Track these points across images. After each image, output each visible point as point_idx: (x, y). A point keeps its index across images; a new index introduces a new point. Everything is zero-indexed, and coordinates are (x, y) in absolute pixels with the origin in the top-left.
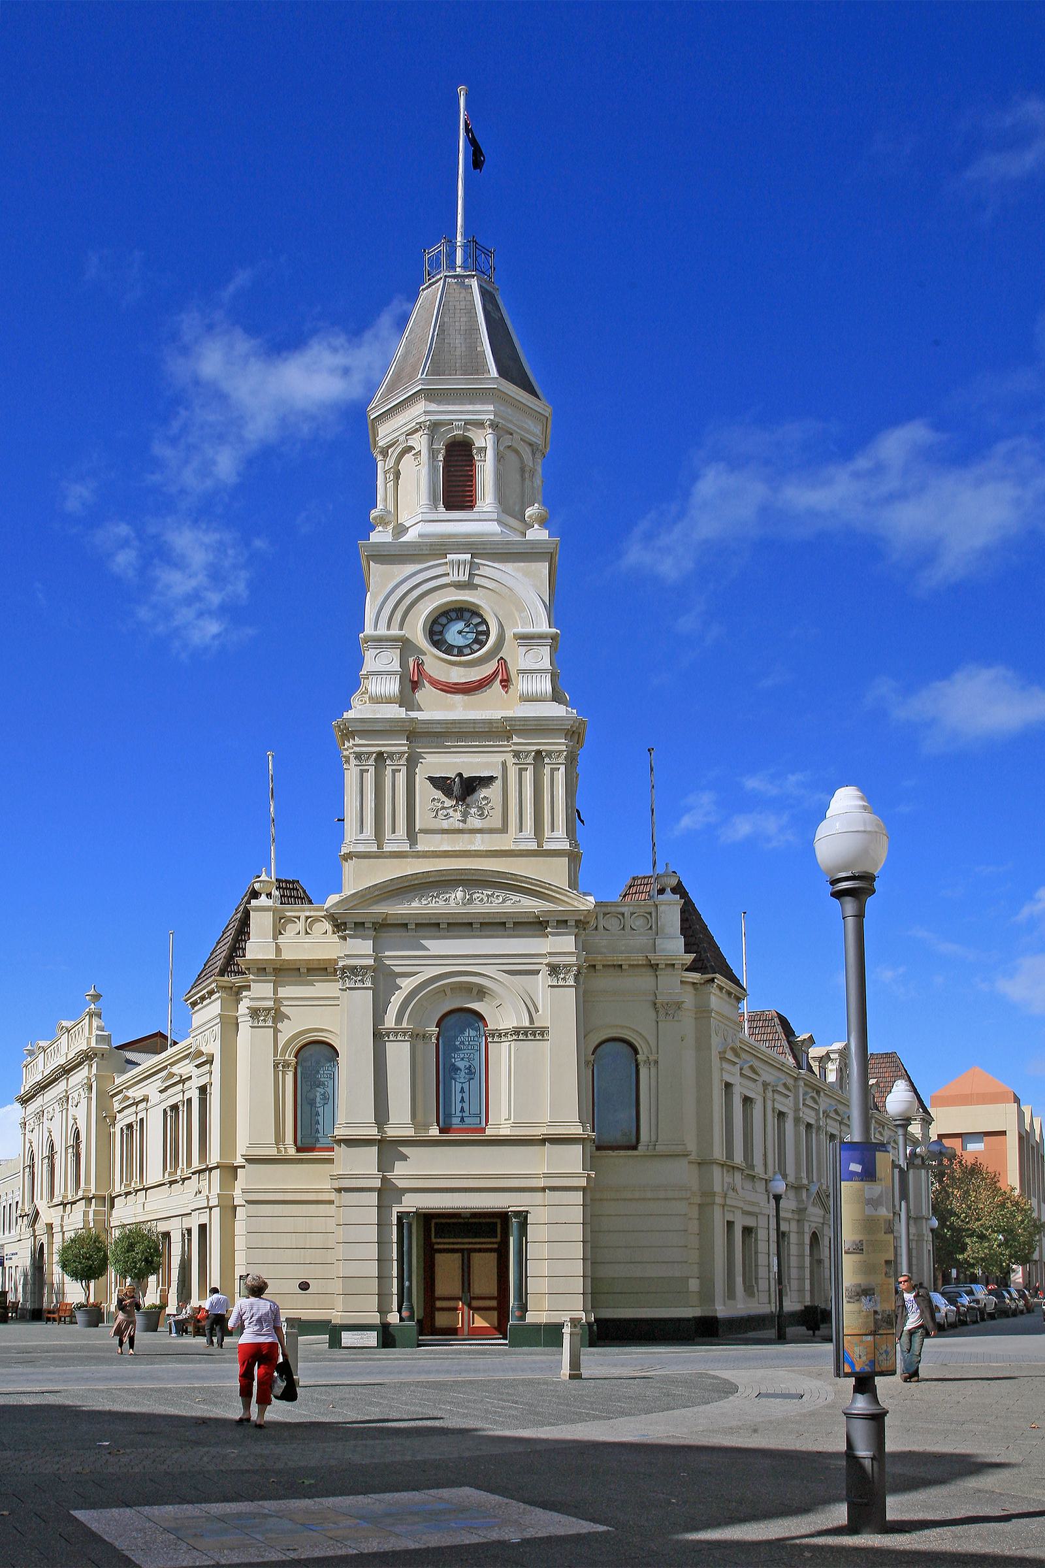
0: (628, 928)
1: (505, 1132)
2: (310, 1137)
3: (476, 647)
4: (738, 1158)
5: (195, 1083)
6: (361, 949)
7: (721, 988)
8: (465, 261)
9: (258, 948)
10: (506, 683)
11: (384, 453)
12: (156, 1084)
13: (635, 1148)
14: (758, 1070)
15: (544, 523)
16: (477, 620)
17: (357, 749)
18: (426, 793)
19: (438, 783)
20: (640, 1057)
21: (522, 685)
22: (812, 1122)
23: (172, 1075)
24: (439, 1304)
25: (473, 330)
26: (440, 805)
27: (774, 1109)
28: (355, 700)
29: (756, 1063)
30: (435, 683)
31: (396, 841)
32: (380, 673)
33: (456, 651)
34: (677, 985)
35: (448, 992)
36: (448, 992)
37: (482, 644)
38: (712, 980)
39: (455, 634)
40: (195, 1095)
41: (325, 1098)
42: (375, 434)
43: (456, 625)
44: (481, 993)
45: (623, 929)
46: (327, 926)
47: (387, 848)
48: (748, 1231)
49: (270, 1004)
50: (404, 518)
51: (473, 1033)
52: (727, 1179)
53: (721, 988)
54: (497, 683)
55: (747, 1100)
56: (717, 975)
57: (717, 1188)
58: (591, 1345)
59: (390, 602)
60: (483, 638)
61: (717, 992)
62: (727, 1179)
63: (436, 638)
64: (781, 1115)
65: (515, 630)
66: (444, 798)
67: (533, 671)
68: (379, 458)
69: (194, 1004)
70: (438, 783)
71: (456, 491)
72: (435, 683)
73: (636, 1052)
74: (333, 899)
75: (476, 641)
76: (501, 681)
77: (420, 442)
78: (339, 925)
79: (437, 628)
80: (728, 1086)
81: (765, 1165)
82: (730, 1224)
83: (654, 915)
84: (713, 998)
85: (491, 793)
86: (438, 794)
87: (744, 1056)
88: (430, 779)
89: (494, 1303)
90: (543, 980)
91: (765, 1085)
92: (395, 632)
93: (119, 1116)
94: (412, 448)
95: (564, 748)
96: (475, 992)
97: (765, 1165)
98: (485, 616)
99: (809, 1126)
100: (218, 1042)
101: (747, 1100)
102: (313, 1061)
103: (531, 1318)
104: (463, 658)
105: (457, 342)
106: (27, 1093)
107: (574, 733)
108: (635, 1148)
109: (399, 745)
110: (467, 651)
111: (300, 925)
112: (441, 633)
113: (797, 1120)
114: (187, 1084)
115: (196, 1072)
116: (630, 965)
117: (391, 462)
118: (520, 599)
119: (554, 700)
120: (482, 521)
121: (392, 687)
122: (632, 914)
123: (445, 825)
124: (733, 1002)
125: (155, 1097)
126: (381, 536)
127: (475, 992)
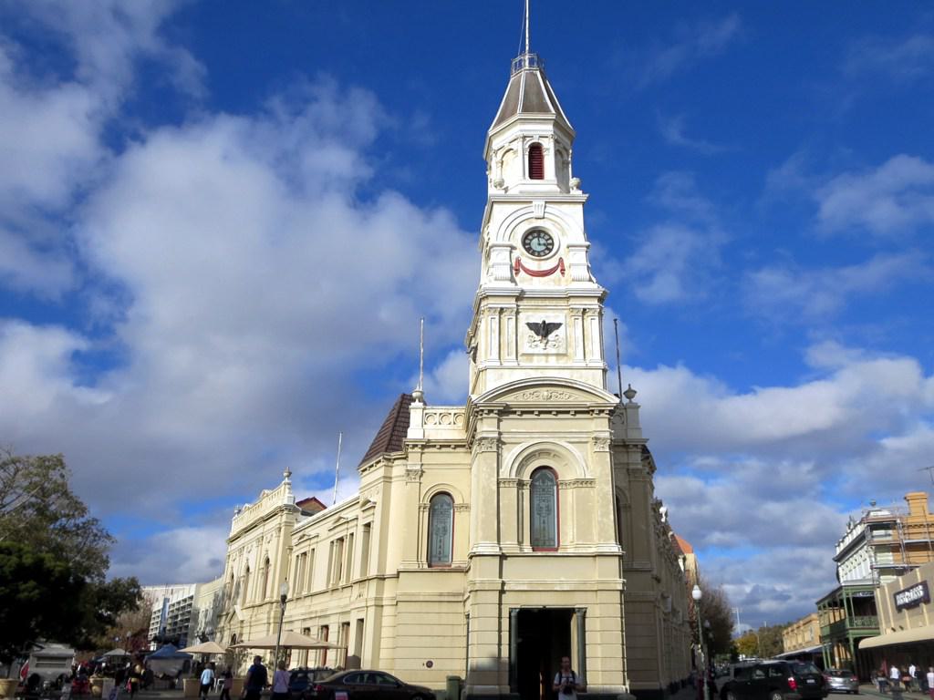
1: (571, 551)
2: (436, 556)
3: (547, 252)
5: (362, 522)
11: (496, 152)
16: (547, 237)
30: (527, 271)
33: (536, 254)
37: (550, 250)
40: (361, 529)
43: (537, 240)
49: (418, 467)
51: (550, 483)
59: (502, 226)
71: (536, 171)
72: (527, 271)
77: (518, 146)
79: (527, 241)
98: (553, 236)
102: (440, 506)
105: (534, 99)
110: (542, 254)
111: (437, 418)
112: (529, 244)
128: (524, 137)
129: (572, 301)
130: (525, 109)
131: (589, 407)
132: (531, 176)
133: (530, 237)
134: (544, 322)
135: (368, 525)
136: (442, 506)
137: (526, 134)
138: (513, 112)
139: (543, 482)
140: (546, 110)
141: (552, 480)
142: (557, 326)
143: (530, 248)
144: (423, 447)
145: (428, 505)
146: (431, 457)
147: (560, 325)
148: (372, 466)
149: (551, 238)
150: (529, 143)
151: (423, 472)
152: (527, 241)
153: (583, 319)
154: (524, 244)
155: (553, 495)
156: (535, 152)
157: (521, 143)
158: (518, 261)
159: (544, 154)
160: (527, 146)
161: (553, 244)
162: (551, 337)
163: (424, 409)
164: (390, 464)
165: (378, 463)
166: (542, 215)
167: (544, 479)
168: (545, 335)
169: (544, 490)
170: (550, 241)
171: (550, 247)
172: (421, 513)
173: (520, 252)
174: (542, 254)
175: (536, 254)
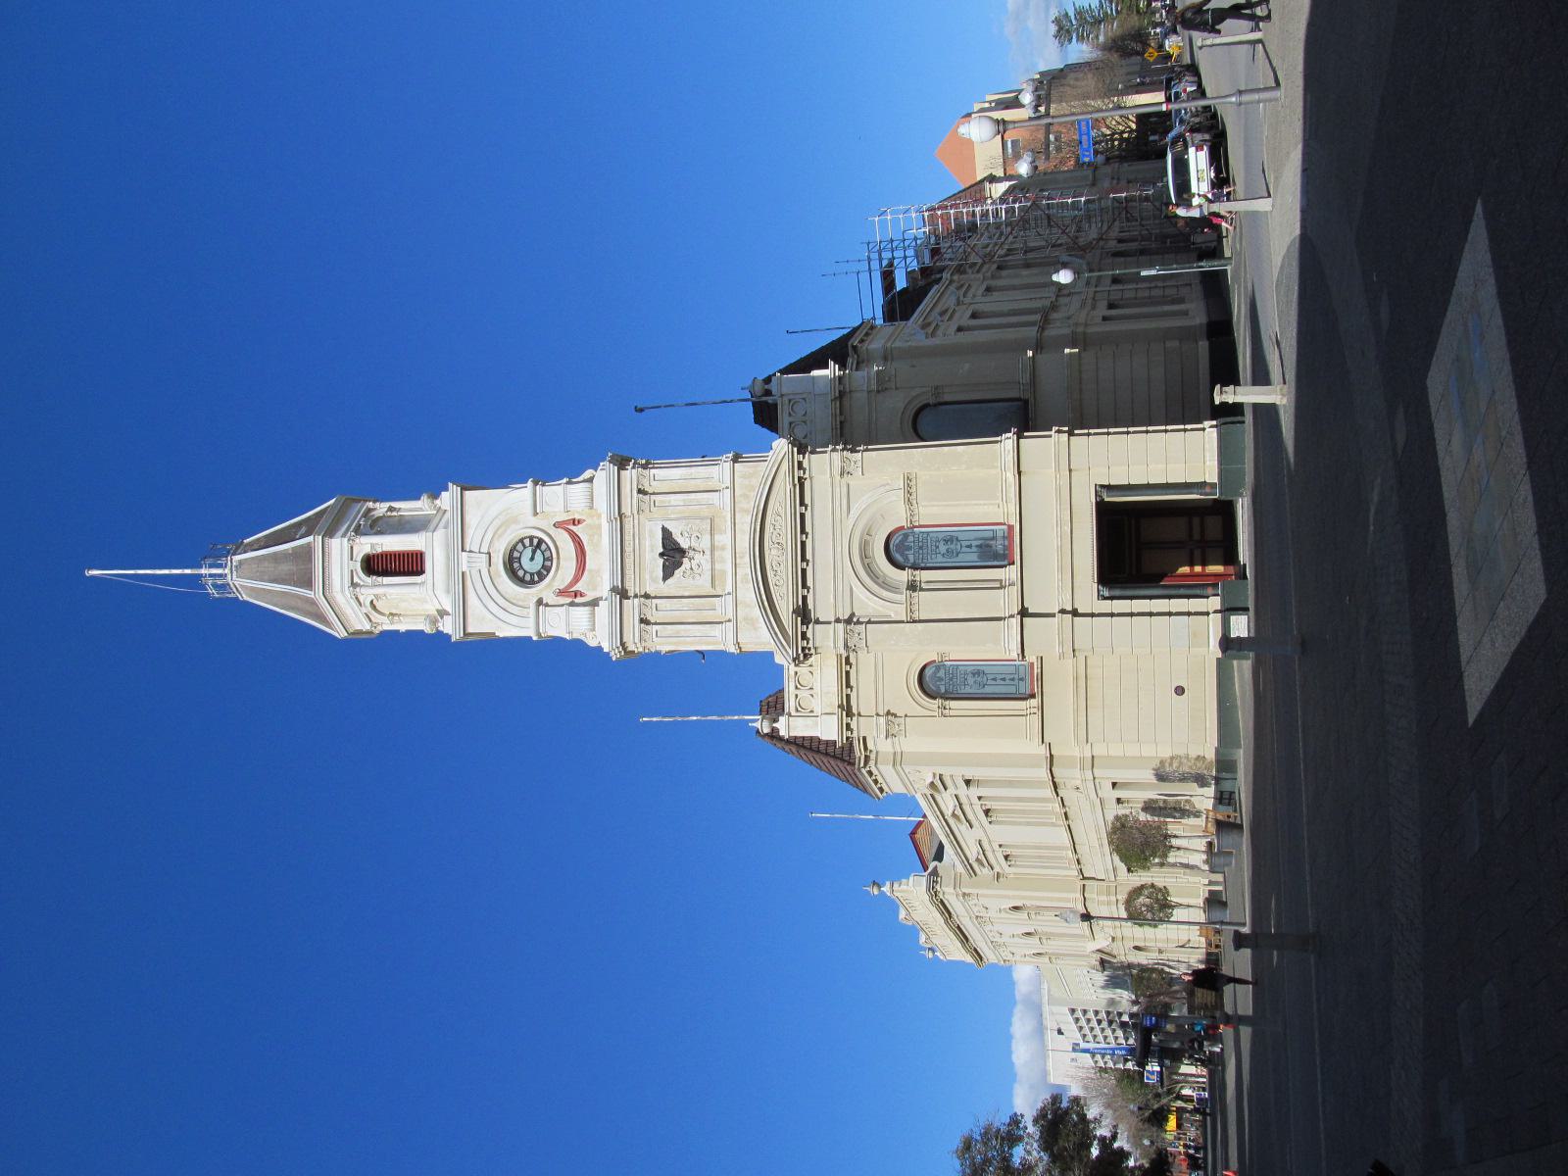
0: (804, 419)
2: (1017, 685)
3: (543, 547)
4: (1037, 317)
5: (962, 790)
6: (827, 639)
7: (862, 341)
8: (220, 566)
9: (827, 729)
10: (574, 522)
12: (961, 829)
13: (1026, 402)
14: (943, 309)
15: (435, 496)
16: (520, 547)
17: (637, 640)
19: (668, 573)
20: (931, 401)
21: (578, 508)
22: (995, 266)
23: (954, 815)
24: (1196, 521)
25: (275, 557)
26: (688, 572)
27: (983, 295)
28: (592, 643)
29: (938, 310)
30: (577, 579)
31: (723, 608)
32: (564, 623)
33: (548, 563)
34: (863, 378)
37: (541, 541)
38: (855, 348)
39: (529, 564)
41: (977, 673)
42: (360, 632)
43: (524, 564)
45: (805, 422)
46: (803, 670)
47: (730, 615)
48: (1111, 306)
49: (882, 720)
50: (431, 609)
51: (911, 538)
52: (1058, 324)
53: (862, 341)
55: (974, 316)
56: (850, 344)
57: (1066, 331)
58: (1243, 403)
59: (505, 615)
61: (866, 344)
62: (1058, 324)
63: (536, 578)
64: (988, 289)
66: (682, 568)
67: (561, 498)
68: (380, 628)
69: (881, 790)
70: (668, 573)
71: (410, 565)
72: (577, 579)
73: (926, 406)
74: (779, 659)
76: (574, 524)
78: (804, 655)
79: (528, 578)
80: (960, 329)
81: (1041, 298)
82: (1105, 319)
83: (791, 397)
84: (873, 346)
86: (678, 573)
87: (930, 319)
88: (665, 578)
89: (1196, 521)
90: (855, 481)
91: (958, 303)
93: (997, 869)
94: (372, 602)
97: (1041, 298)
98: (517, 539)
99: (999, 268)
100: (918, 768)
101: (974, 316)
103: (1212, 476)
104: (555, 555)
105: (285, 568)
106: (973, 956)
107: (622, 463)
108: (1026, 402)
110: (547, 554)
111: (803, 694)
112: (532, 574)
113: (993, 277)
114: (964, 800)
115: (951, 790)
116: (841, 414)
117: (384, 619)
118: (501, 512)
119: (592, 481)
120: (431, 544)
121: (582, 613)
122: (790, 415)
123: (707, 566)
124: (874, 332)
125: (978, 833)
126: (447, 626)
128: (354, 585)
129: (626, 510)
130: (308, 584)
131: (794, 486)
132: (421, 572)
133: (521, 573)
134: (662, 555)
135: (968, 782)
136: (940, 679)
137: (347, 582)
138: (313, 602)
139: (910, 548)
140: (308, 551)
141: (906, 536)
142: (667, 535)
143: (539, 573)
144: (850, 714)
145: (938, 702)
146: (863, 701)
147: (664, 529)
148: (876, 782)
149: (521, 541)
150: (361, 577)
151: (888, 713)
152: (528, 578)
153: (654, 494)
154: (532, 582)
155: (928, 533)
156: (375, 565)
157: (363, 590)
158: (562, 593)
159: (379, 550)
160: (369, 580)
161: (531, 538)
162: (684, 544)
163: (790, 715)
164: (873, 756)
165: (870, 773)
166: (485, 557)
167: (903, 547)
168: (682, 552)
169: (921, 548)
170: (527, 542)
171: (535, 541)
172: (952, 713)
173: (545, 590)
174: (547, 554)
175: (548, 563)
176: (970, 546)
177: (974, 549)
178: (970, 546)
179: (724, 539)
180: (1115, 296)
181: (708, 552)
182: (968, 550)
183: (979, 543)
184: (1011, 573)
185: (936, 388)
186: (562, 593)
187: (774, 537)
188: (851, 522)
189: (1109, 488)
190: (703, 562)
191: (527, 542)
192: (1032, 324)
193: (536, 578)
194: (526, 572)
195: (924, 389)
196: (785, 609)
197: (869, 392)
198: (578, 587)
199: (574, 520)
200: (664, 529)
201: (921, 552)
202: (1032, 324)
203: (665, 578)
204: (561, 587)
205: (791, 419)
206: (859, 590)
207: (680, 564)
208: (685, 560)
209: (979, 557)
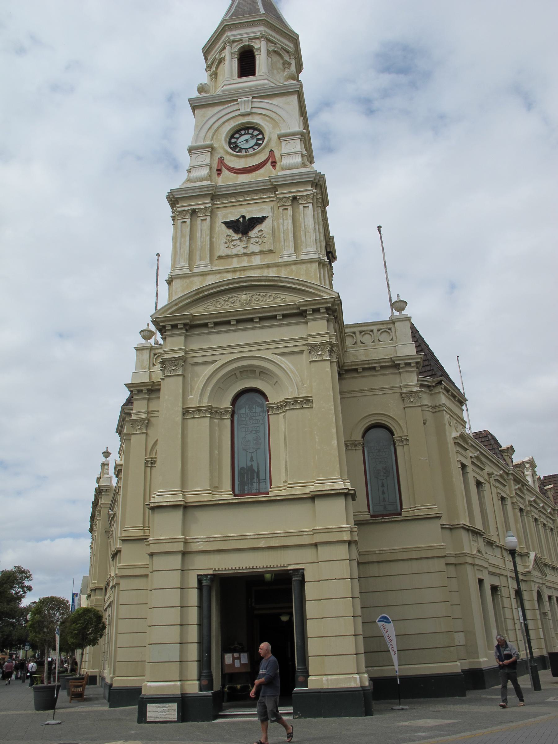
3: (256, 147)
10: (274, 164)
18: (223, 231)
30: (231, 169)
35: (238, 375)
36: (238, 375)
39: (242, 140)
44: (263, 373)
47: (196, 270)
54: (269, 163)
60: (260, 142)
63: (232, 146)
65: (279, 132)
72: (231, 169)
75: (257, 144)
76: (272, 163)
79: (233, 140)
85: (265, 227)
86: (230, 232)
88: (226, 223)
92: (209, 142)
95: (310, 192)
96: (258, 372)
109: (207, 203)
123: (235, 251)
127: (258, 372)
133: (237, 136)
143: (237, 146)
150: (236, 48)
158: (221, 160)
161: (263, 139)
169: (251, 418)
170: (261, 136)
176: (252, 460)
177: (249, 464)
178: (252, 460)
179: (257, 260)
180: (504, 592)
181: (246, 251)
182: (249, 458)
183: (255, 468)
184: (226, 495)
185: (407, 440)
186: (221, 160)
187: (257, 296)
188: (271, 357)
189: (302, 582)
190: (238, 248)
191: (261, 136)
192: (471, 517)
193: (232, 146)
194: (237, 139)
195: (405, 430)
196: (199, 310)
197: (400, 387)
198: (225, 172)
199: (275, 162)
200: (264, 219)
201: (247, 419)
202: (471, 517)
203: (226, 223)
204: (225, 161)
205: (375, 331)
206: (212, 368)
207: (236, 231)
208: (240, 236)
209: (243, 468)
